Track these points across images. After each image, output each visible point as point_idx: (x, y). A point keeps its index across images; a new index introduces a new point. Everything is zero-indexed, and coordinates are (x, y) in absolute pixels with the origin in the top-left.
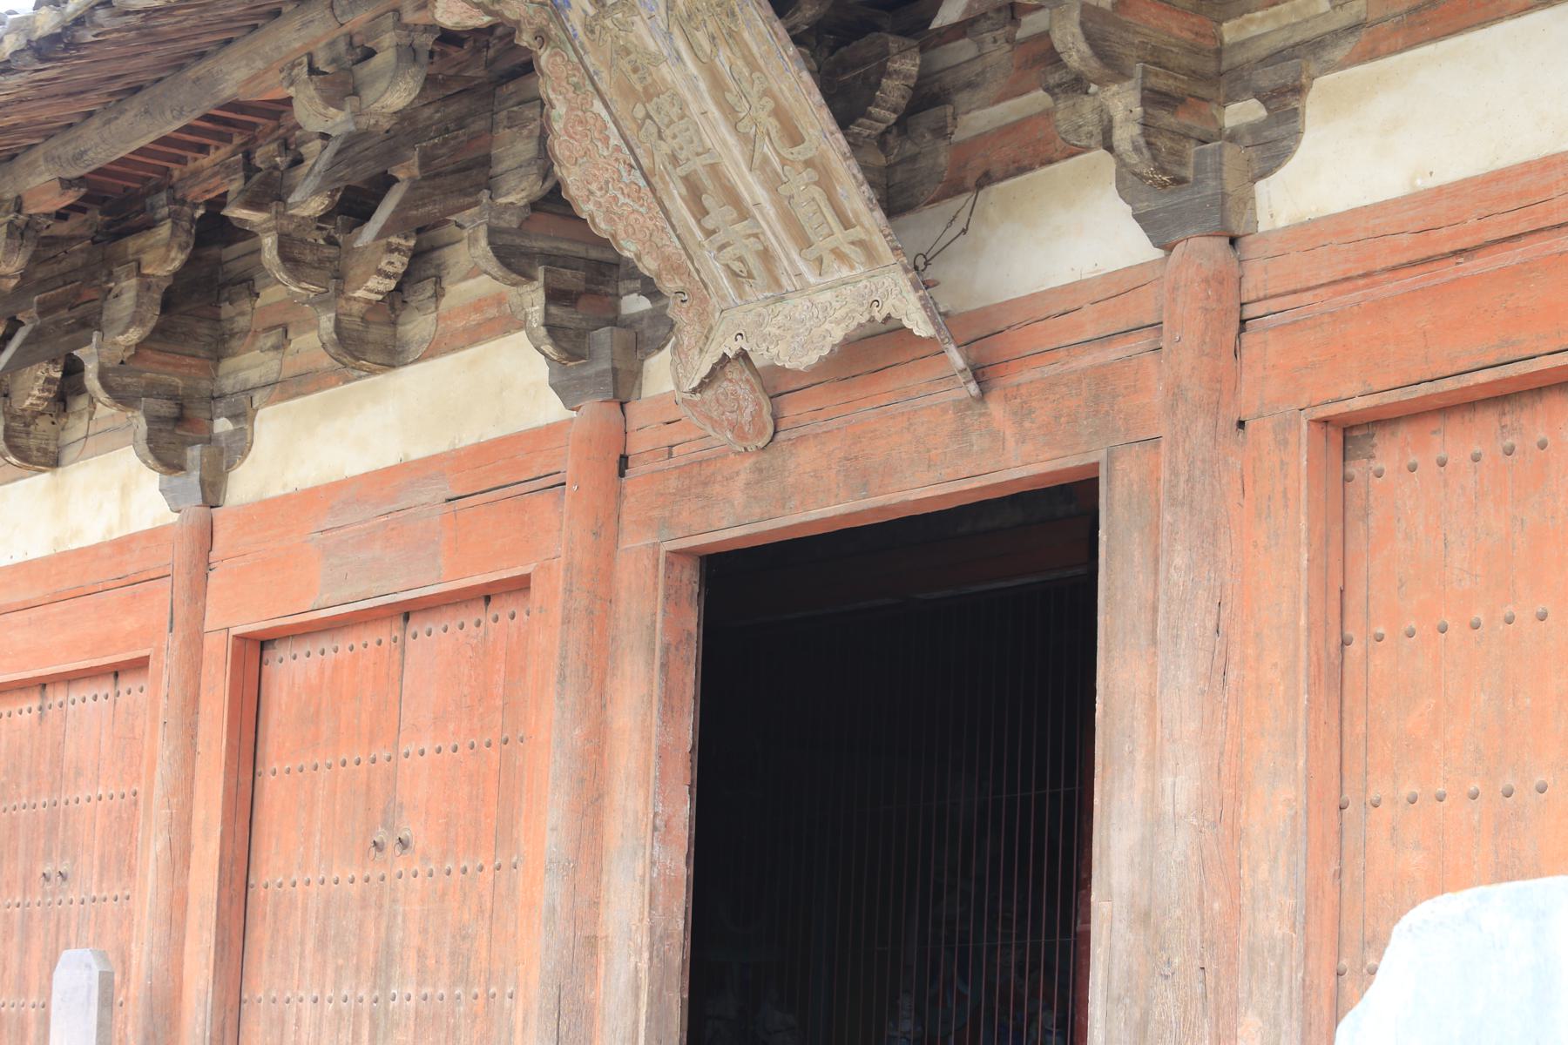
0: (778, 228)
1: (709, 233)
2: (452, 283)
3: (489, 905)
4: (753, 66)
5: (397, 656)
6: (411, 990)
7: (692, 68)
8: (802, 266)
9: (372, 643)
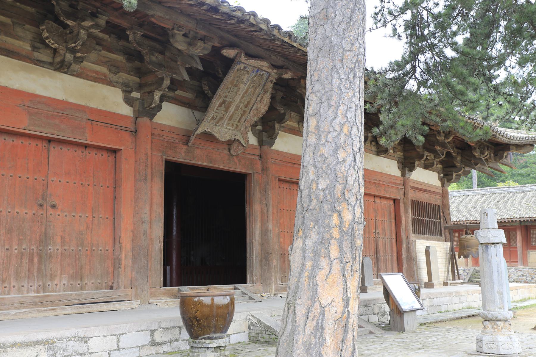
0: (229, 116)
1: (217, 109)
2: (86, 61)
3: (91, 226)
4: (253, 94)
5: (46, 151)
6: (58, 247)
7: (246, 88)
8: (225, 123)
9: (20, 142)
